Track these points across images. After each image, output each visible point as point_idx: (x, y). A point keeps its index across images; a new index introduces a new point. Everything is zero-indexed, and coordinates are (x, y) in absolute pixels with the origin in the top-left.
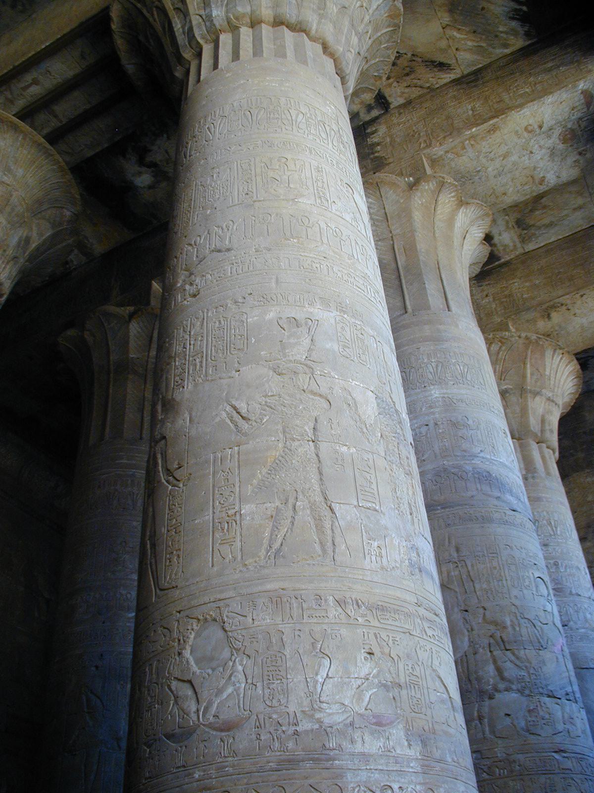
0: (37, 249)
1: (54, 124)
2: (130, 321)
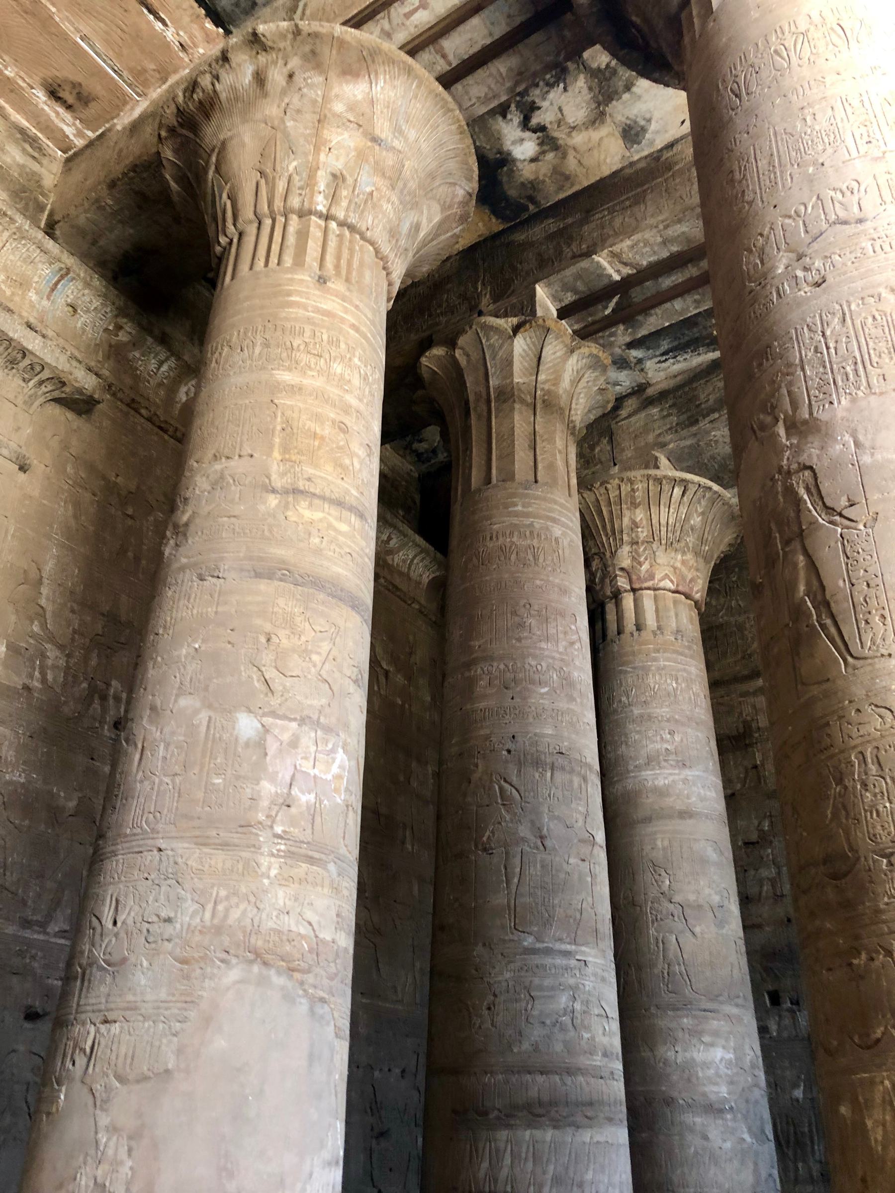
1: (442, 67)
2: (515, 335)
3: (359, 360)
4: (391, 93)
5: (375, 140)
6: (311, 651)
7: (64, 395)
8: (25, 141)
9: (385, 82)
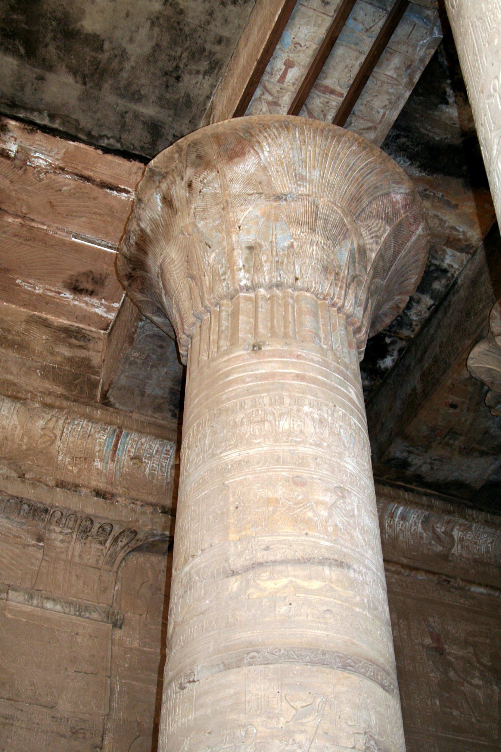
0: (381, 256)
3: (311, 405)
4: (279, 152)
5: (279, 198)
6: (294, 732)
7: (140, 543)
8: (70, 337)
9: (269, 146)
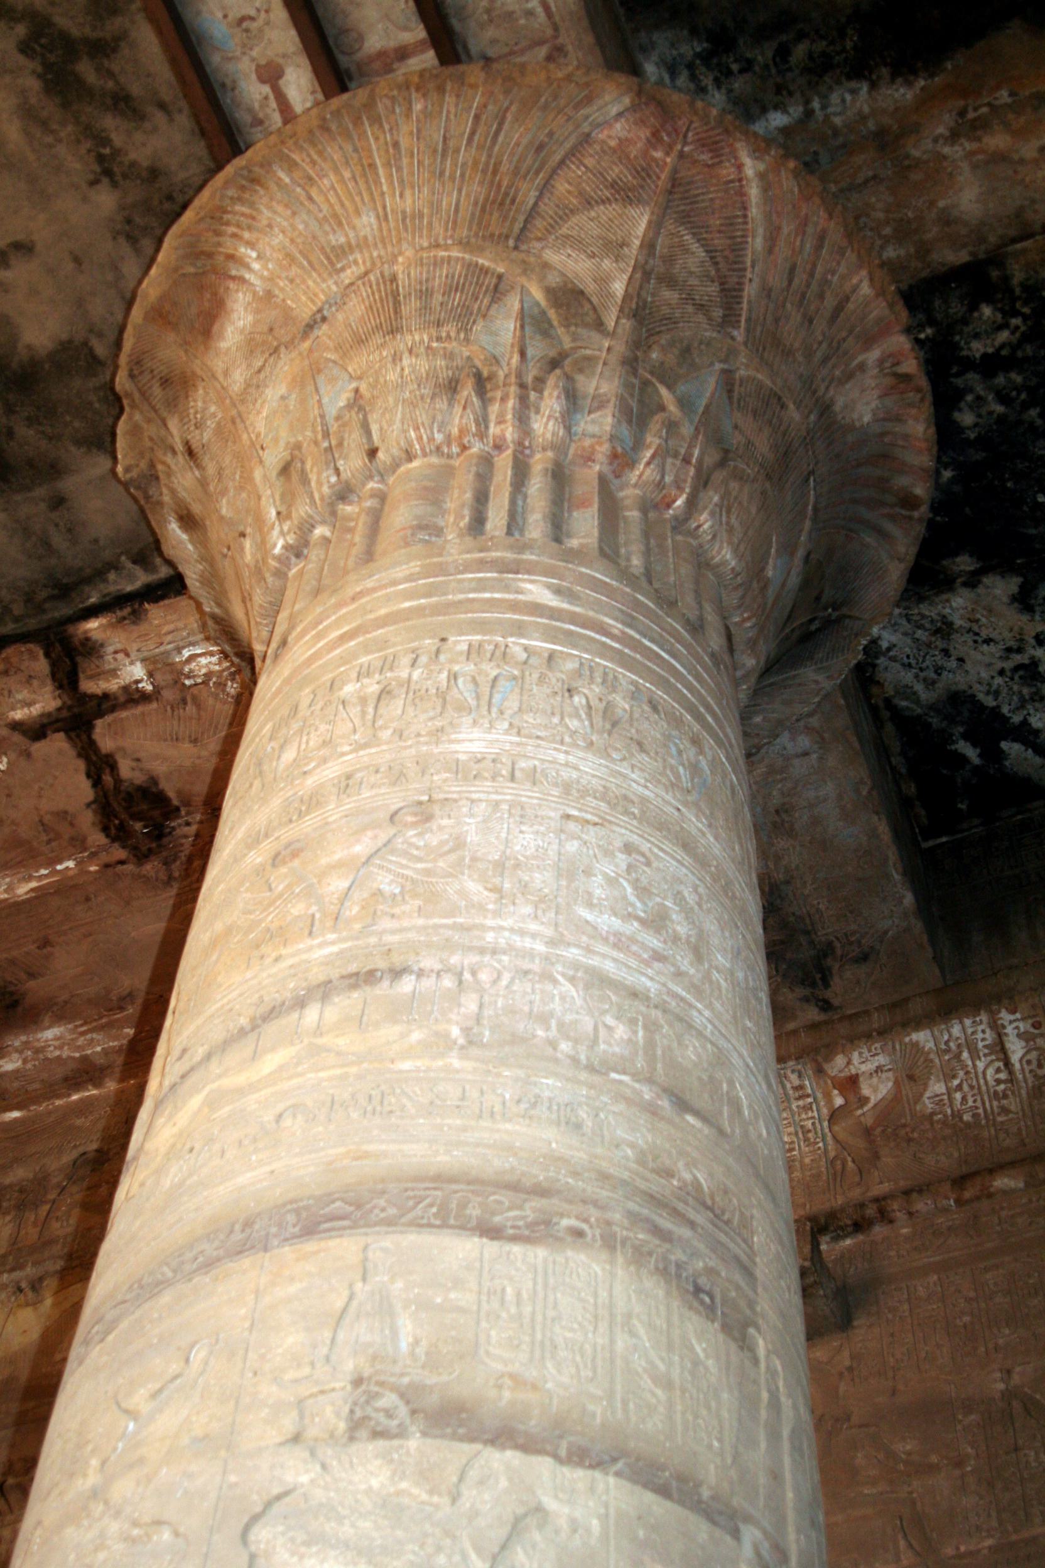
4: (275, 242)
9: (251, 245)
